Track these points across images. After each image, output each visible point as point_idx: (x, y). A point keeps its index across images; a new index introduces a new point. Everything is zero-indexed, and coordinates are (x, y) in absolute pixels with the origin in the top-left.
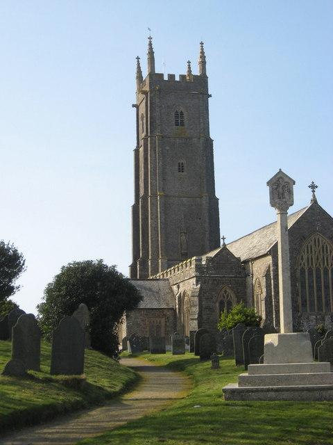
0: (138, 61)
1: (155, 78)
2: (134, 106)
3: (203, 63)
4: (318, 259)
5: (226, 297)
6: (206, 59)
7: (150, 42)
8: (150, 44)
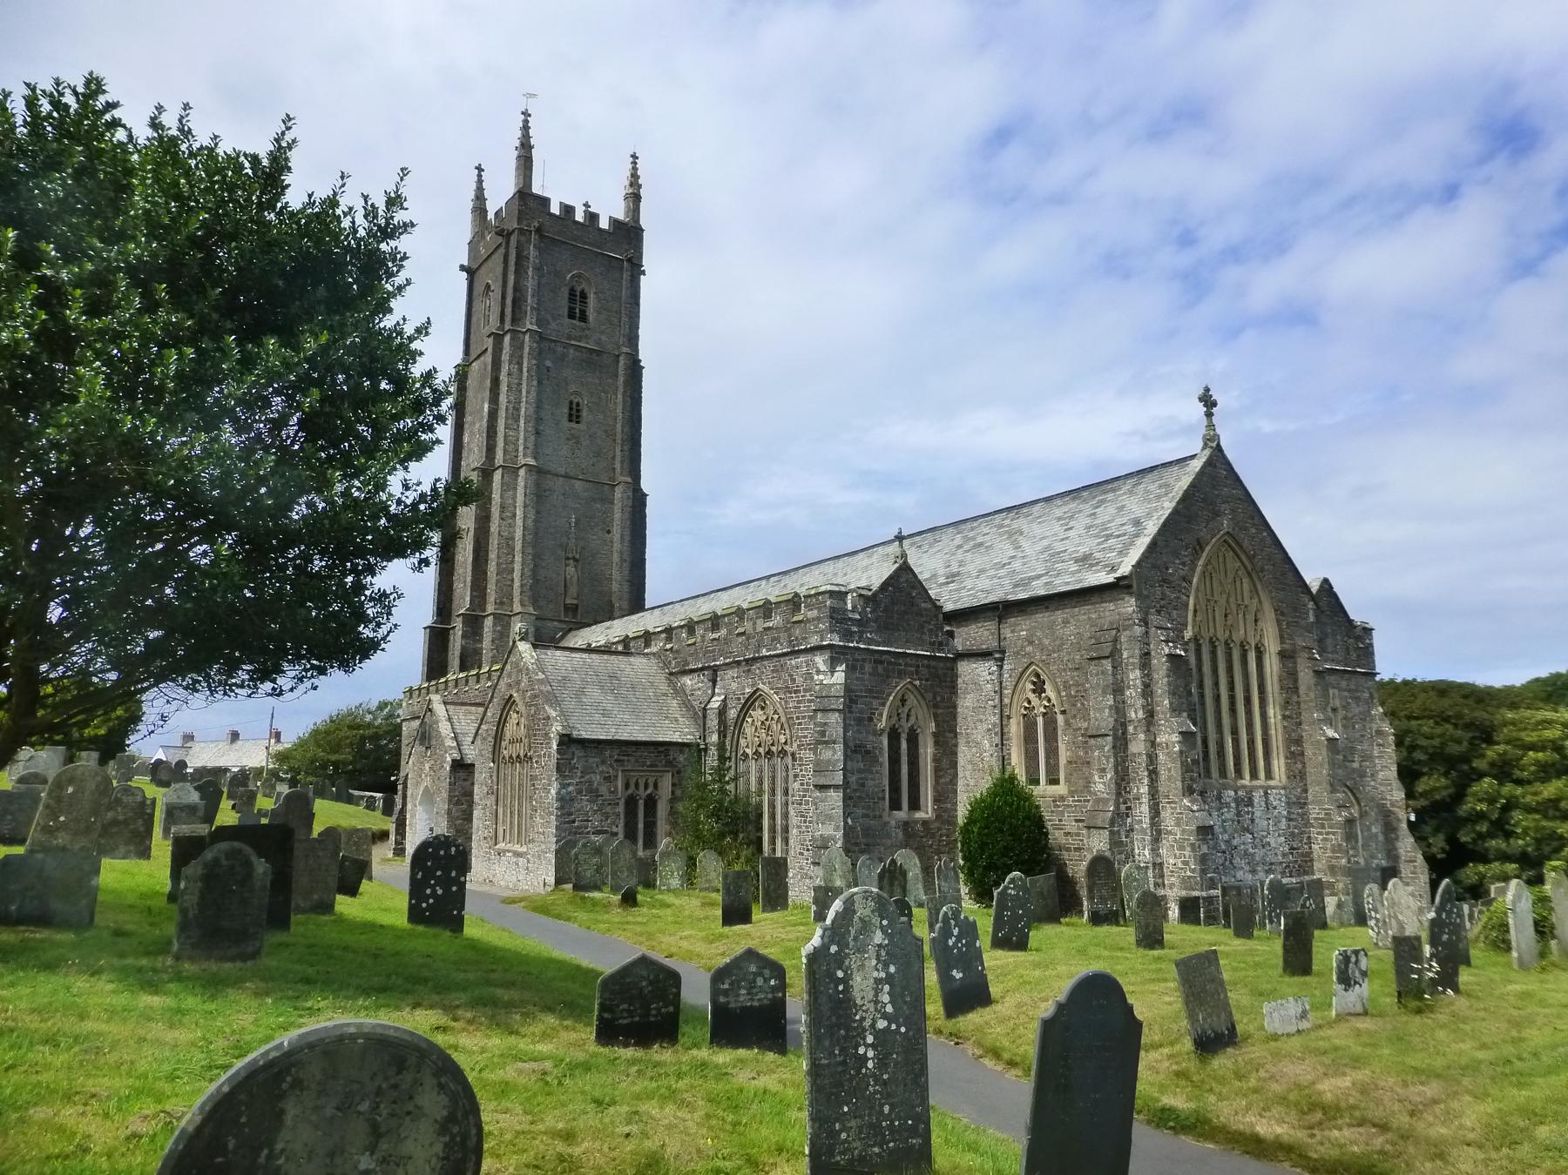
0: (480, 176)
1: (527, 201)
2: (462, 268)
3: (634, 198)
4: (1226, 616)
5: (904, 716)
6: (642, 192)
7: (526, 122)
8: (526, 128)
